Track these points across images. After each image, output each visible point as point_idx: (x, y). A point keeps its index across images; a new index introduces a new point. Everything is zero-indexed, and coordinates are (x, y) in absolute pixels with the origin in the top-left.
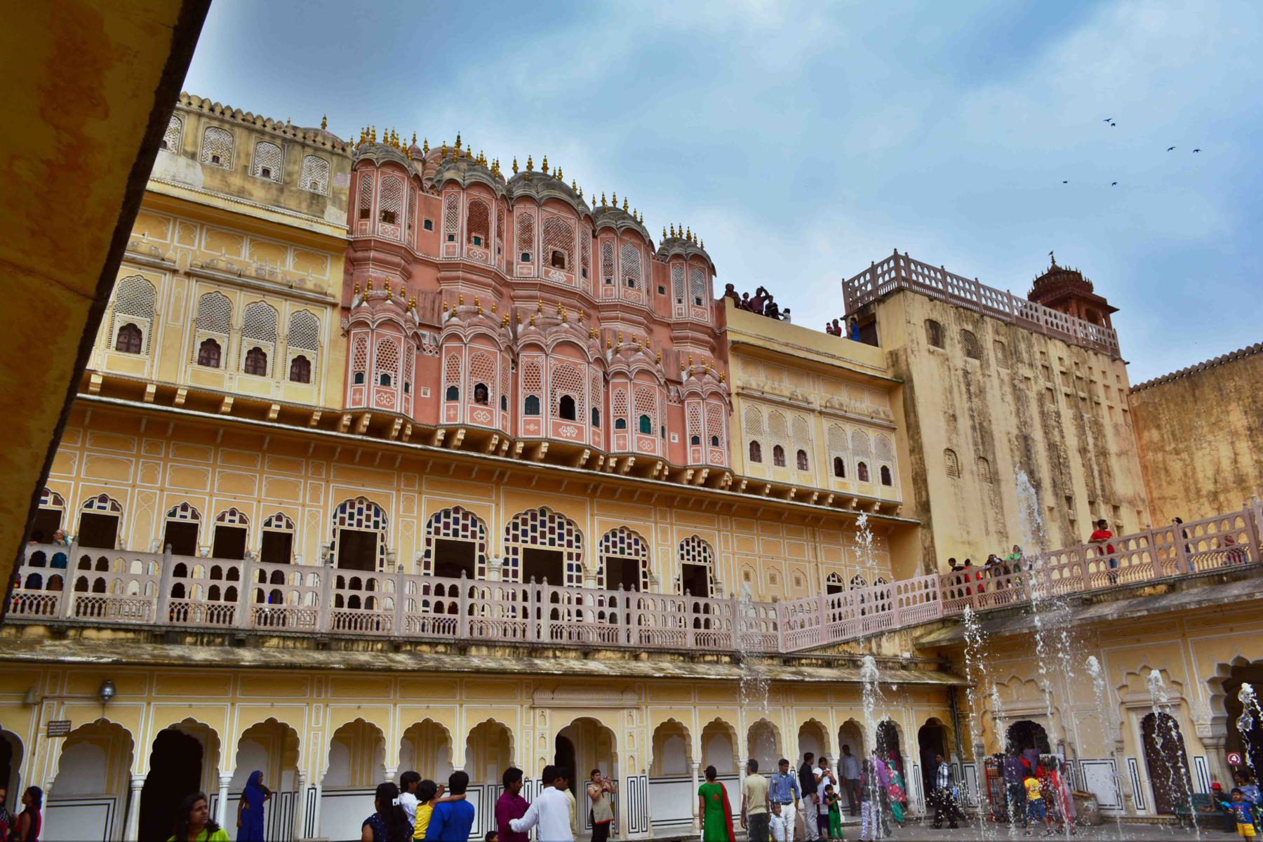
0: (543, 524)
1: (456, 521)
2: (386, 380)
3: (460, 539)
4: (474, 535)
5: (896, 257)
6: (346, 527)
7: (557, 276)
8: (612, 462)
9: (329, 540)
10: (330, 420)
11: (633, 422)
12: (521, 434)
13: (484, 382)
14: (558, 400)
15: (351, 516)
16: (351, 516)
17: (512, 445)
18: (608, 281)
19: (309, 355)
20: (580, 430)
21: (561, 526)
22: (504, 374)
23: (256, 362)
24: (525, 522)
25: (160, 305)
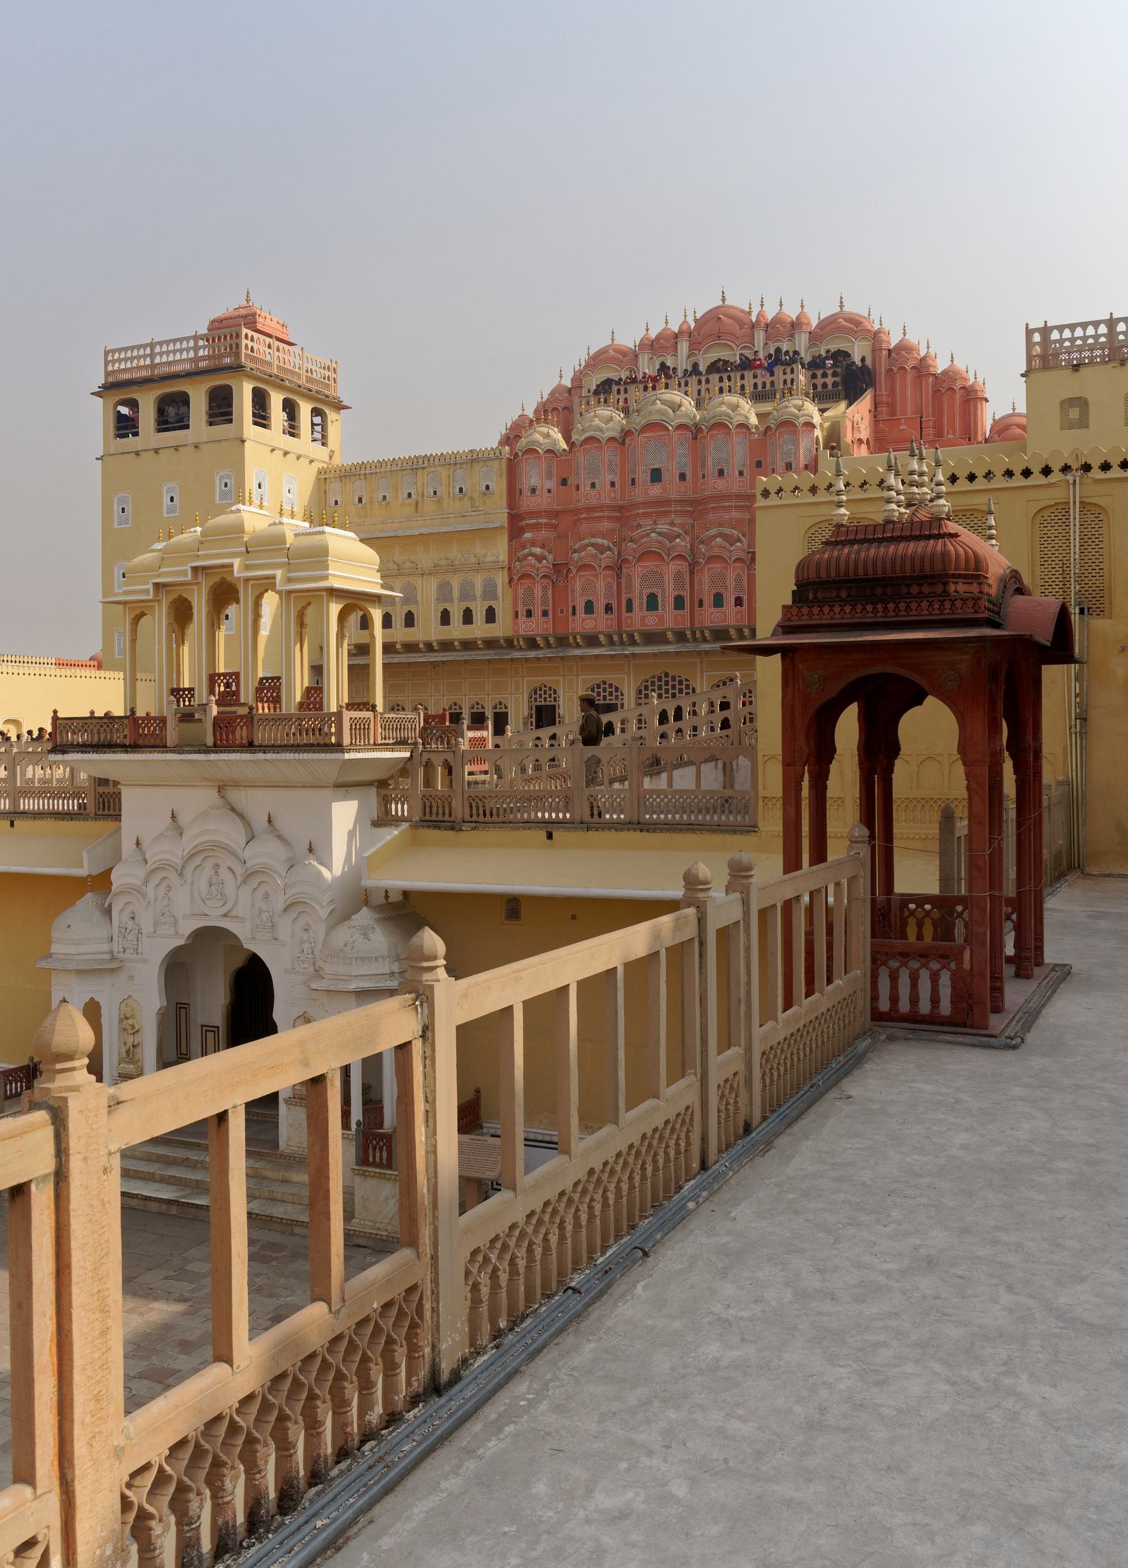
0: (667, 683)
1: (605, 690)
2: (529, 614)
3: (608, 702)
4: (617, 698)
5: (1029, 333)
6: (538, 703)
7: (655, 491)
8: (698, 635)
9: (526, 713)
10: (510, 643)
11: (708, 600)
12: (624, 628)
13: (590, 598)
14: (645, 600)
15: (540, 696)
16: (540, 696)
17: (621, 636)
18: (704, 477)
19: (493, 604)
20: (661, 618)
21: (681, 682)
22: (608, 586)
23: (468, 617)
24: (653, 684)
25: (419, 598)
